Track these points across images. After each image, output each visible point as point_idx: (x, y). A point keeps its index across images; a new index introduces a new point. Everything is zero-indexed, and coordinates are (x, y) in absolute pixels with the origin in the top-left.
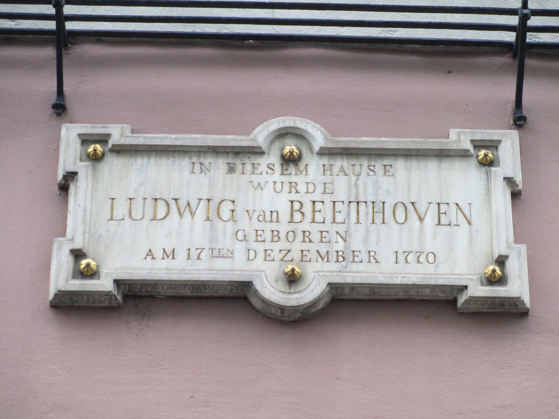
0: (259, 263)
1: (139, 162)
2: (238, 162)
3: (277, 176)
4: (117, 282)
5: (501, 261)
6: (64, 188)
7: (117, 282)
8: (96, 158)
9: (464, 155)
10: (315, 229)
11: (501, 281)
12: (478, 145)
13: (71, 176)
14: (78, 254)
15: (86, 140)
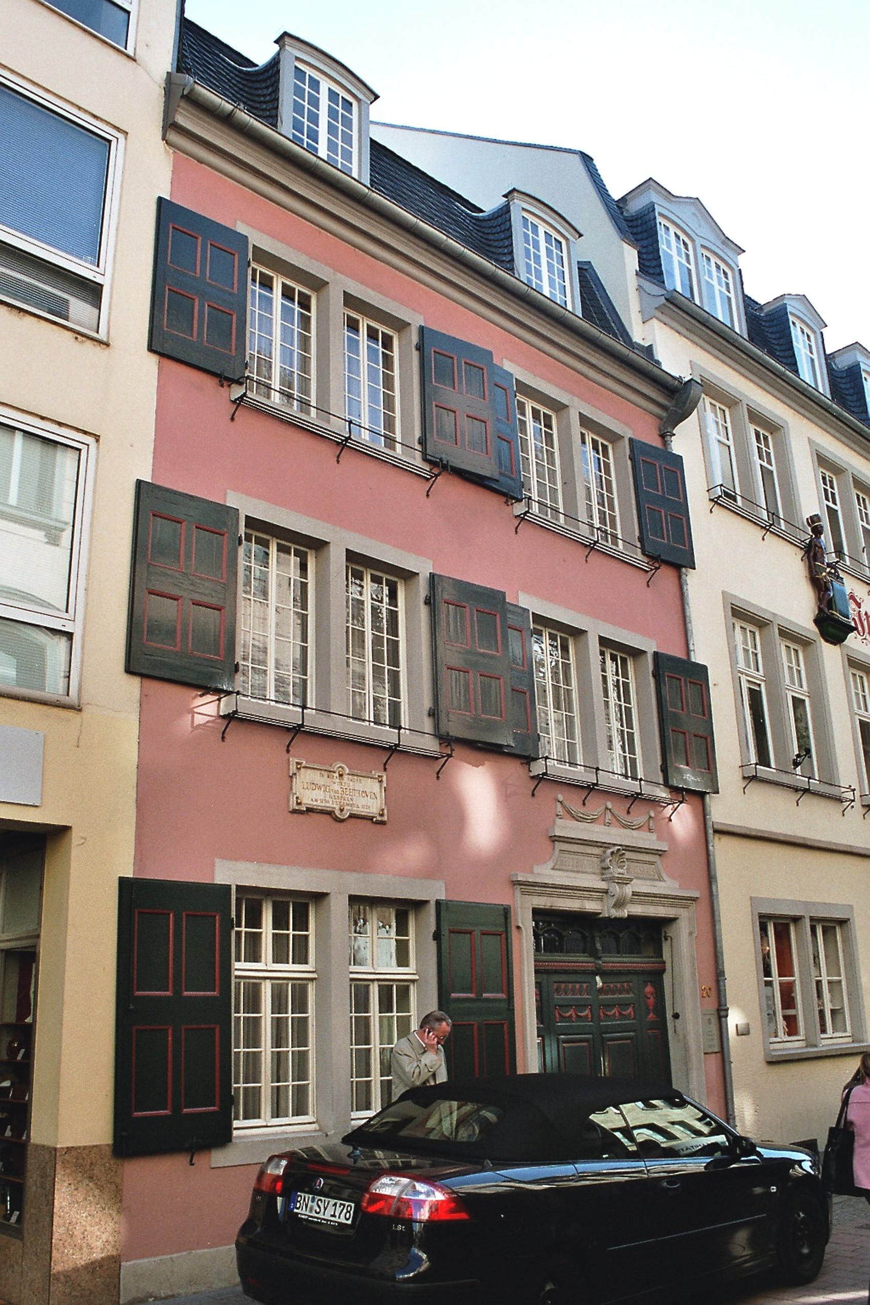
0: (334, 806)
1: (309, 771)
2: (330, 774)
3: (338, 780)
4: (307, 808)
5: (383, 810)
6: (291, 777)
7: (307, 808)
8: (299, 769)
9: (376, 778)
10: (346, 796)
11: (382, 815)
12: (379, 776)
13: (295, 774)
14: (297, 798)
15: (298, 763)
